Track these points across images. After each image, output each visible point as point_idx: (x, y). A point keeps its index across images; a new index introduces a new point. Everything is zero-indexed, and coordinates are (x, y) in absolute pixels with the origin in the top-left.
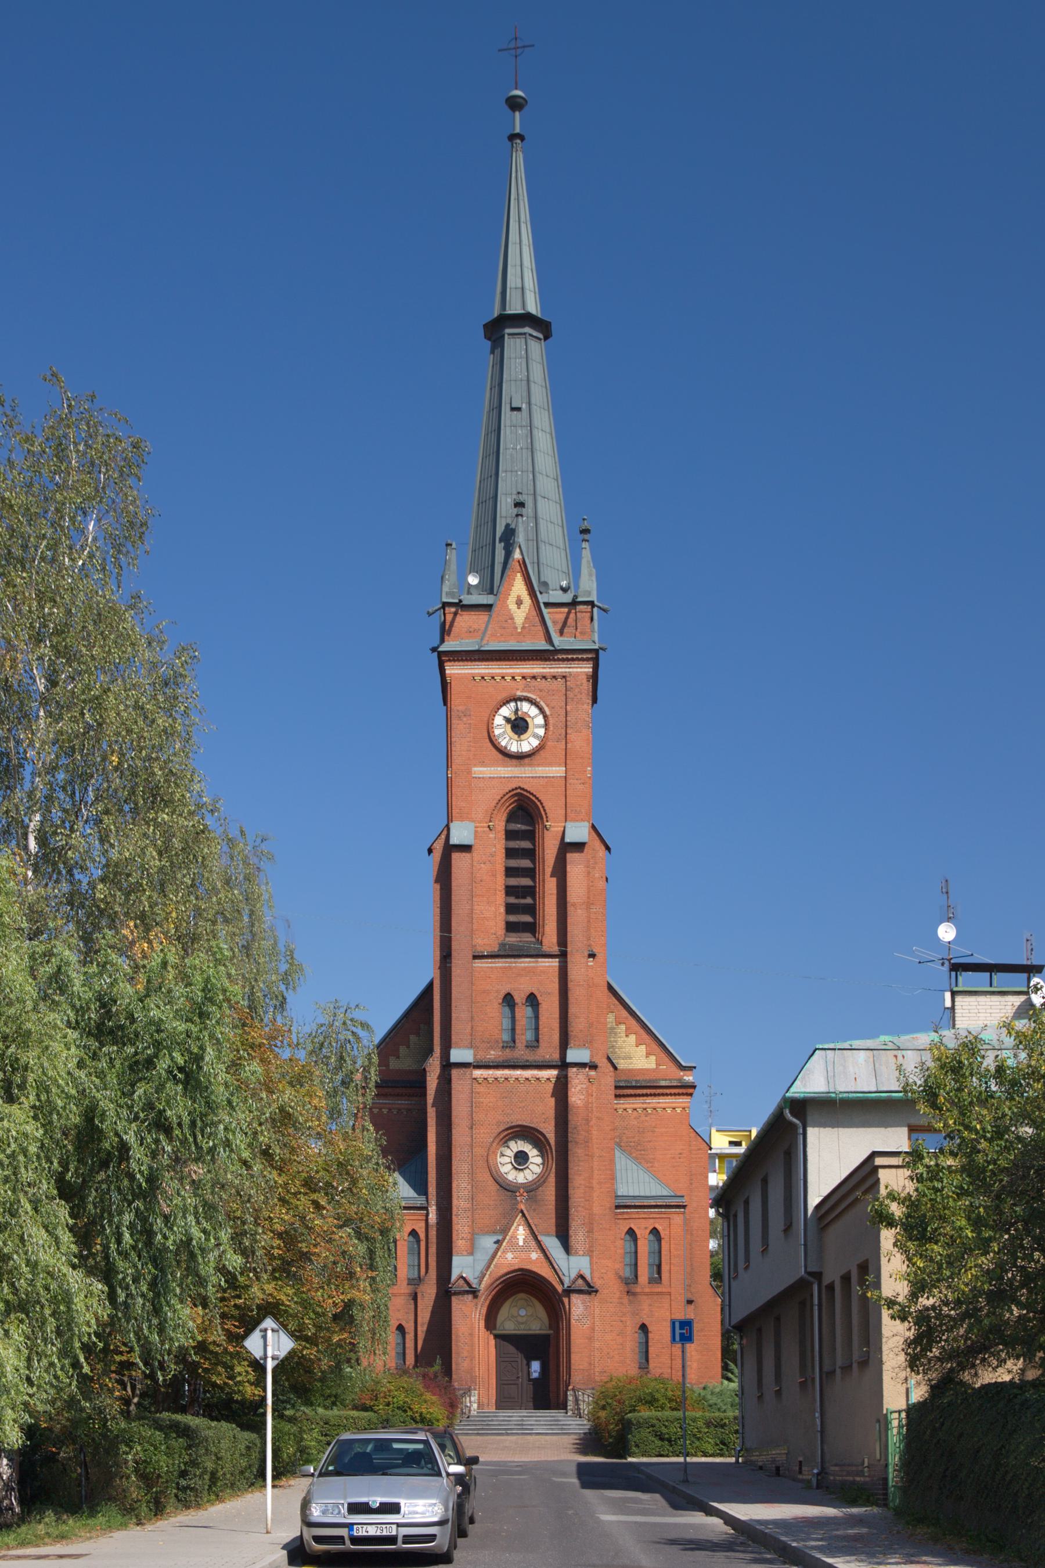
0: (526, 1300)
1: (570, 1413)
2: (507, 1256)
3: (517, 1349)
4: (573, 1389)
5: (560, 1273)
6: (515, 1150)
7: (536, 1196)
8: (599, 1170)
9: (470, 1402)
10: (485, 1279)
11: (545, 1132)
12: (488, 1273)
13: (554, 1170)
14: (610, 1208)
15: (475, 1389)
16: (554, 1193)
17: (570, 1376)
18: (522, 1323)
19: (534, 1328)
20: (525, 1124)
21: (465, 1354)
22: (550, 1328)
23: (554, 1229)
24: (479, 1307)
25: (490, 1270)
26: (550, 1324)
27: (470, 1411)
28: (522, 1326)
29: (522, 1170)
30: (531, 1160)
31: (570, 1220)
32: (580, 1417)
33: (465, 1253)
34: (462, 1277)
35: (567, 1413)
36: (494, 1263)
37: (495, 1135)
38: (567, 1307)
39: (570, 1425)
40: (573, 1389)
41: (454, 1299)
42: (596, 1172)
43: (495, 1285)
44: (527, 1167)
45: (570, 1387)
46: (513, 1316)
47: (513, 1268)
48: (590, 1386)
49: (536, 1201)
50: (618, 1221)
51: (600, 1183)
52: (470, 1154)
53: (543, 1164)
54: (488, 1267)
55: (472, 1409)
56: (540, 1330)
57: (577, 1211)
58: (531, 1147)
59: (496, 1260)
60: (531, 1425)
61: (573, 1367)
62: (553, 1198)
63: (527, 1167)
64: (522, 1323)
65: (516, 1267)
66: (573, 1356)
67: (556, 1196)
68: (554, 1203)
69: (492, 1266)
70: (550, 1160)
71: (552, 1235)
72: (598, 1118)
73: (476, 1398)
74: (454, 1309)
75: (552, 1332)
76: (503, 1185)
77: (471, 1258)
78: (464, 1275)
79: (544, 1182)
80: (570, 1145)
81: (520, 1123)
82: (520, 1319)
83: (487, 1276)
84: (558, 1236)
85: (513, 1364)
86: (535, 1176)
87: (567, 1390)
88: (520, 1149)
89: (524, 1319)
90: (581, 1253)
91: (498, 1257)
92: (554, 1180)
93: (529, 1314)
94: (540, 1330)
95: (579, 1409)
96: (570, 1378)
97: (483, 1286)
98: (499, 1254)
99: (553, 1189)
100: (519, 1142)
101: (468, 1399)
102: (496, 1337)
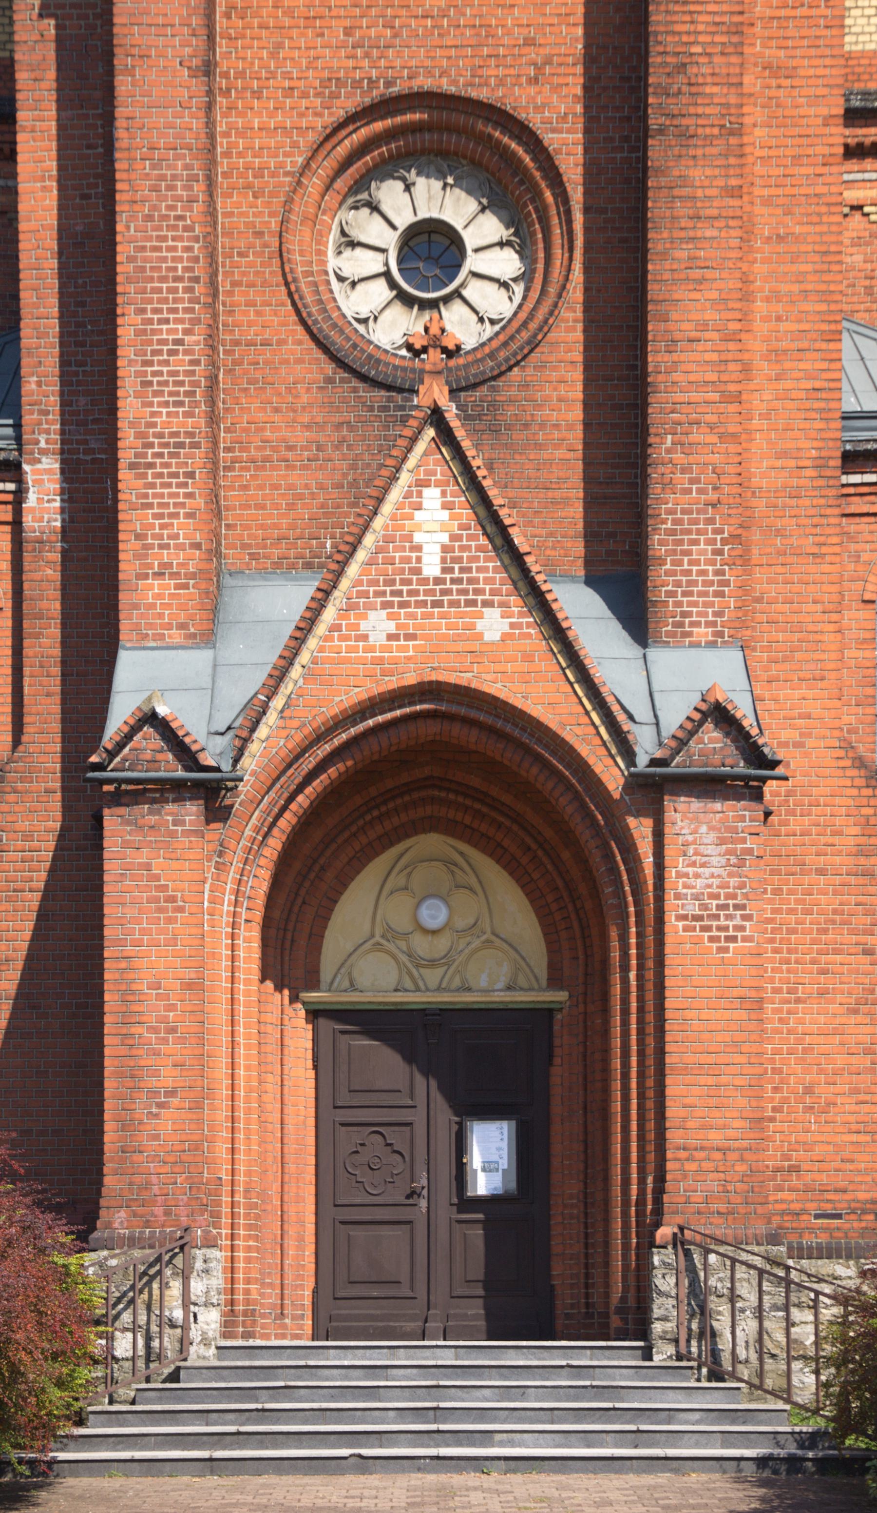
0: (449, 863)
1: (663, 1354)
2: (364, 626)
3: (409, 1058)
4: (678, 1241)
5: (621, 717)
6: (404, 219)
7: (494, 406)
8: (774, 297)
9: (186, 1302)
10: (262, 731)
11: (536, 122)
12: (278, 702)
13: (576, 292)
14: (820, 464)
15: (210, 1243)
16: (577, 393)
17: (661, 1179)
18: (433, 963)
19: (483, 982)
20: (446, 86)
21: (167, 1078)
22: (555, 981)
23: (579, 548)
24: (237, 864)
25: (287, 688)
26: (553, 967)
27: (184, 1343)
28: (432, 977)
29: (433, 304)
30: (473, 262)
31: (655, 489)
32: (716, 1375)
33: (176, 636)
34: (151, 718)
35: (647, 1354)
36: (304, 657)
37: (312, 137)
38: (649, 869)
39: (672, 1413)
40: (678, 1241)
41: (112, 820)
42: (760, 306)
43: (309, 762)
44: (457, 294)
45: (664, 1232)
46: (391, 934)
47: (392, 683)
48: (762, 1229)
49: (495, 431)
50: (852, 526)
51: (776, 355)
52: (199, 188)
53: (526, 277)
54: (279, 675)
55: (195, 1334)
56: (509, 988)
57: (688, 448)
58: (471, 205)
59: (312, 643)
60: (482, 1413)
61: (674, 1137)
62: (577, 414)
63: (457, 294)
64: (433, 963)
65: (411, 679)
66: (674, 1087)
67: (587, 406)
68: (577, 436)
69: (296, 672)
70: (557, 251)
71: (573, 579)
72: (772, 69)
73: (217, 1280)
74: (112, 868)
75: (562, 996)
76: (352, 358)
77: (202, 658)
78: (162, 710)
79: (533, 345)
80: (656, 150)
81: (425, 83)
82: (422, 945)
83: (271, 717)
84: (590, 581)
85: (393, 1136)
86: (489, 330)
87: (648, 1244)
88: (423, 214)
89: (442, 944)
90: (703, 633)
91: (321, 629)
92: (579, 335)
93: (461, 923)
94: (509, 988)
95: (709, 1334)
96: (660, 1191)
97: (248, 763)
98: (329, 615)
99: (577, 375)
100: (422, 184)
101: (176, 1287)
102: (314, 1014)
